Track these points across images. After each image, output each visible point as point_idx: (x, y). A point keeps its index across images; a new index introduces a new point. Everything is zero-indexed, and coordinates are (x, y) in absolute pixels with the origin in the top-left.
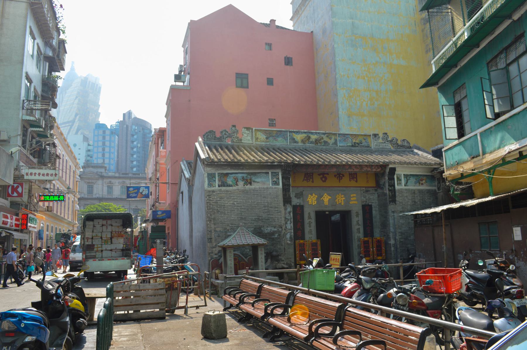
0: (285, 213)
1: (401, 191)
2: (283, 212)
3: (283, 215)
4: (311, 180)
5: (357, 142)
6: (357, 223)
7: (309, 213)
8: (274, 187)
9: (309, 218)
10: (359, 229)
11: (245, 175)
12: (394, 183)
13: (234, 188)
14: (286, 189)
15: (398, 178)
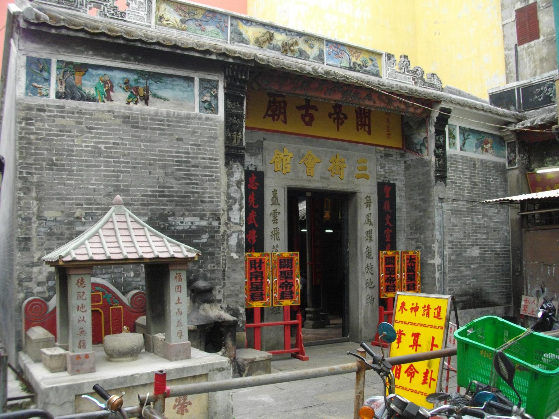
0: (229, 186)
1: (453, 157)
2: (224, 180)
3: (223, 188)
4: (282, 117)
5: (359, 62)
7: (275, 191)
8: (204, 115)
9: (275, 201)
10: (369, 233)
11: (132, 77)
12: (444, 141)
14: (232, 125)
15: (450, 133)
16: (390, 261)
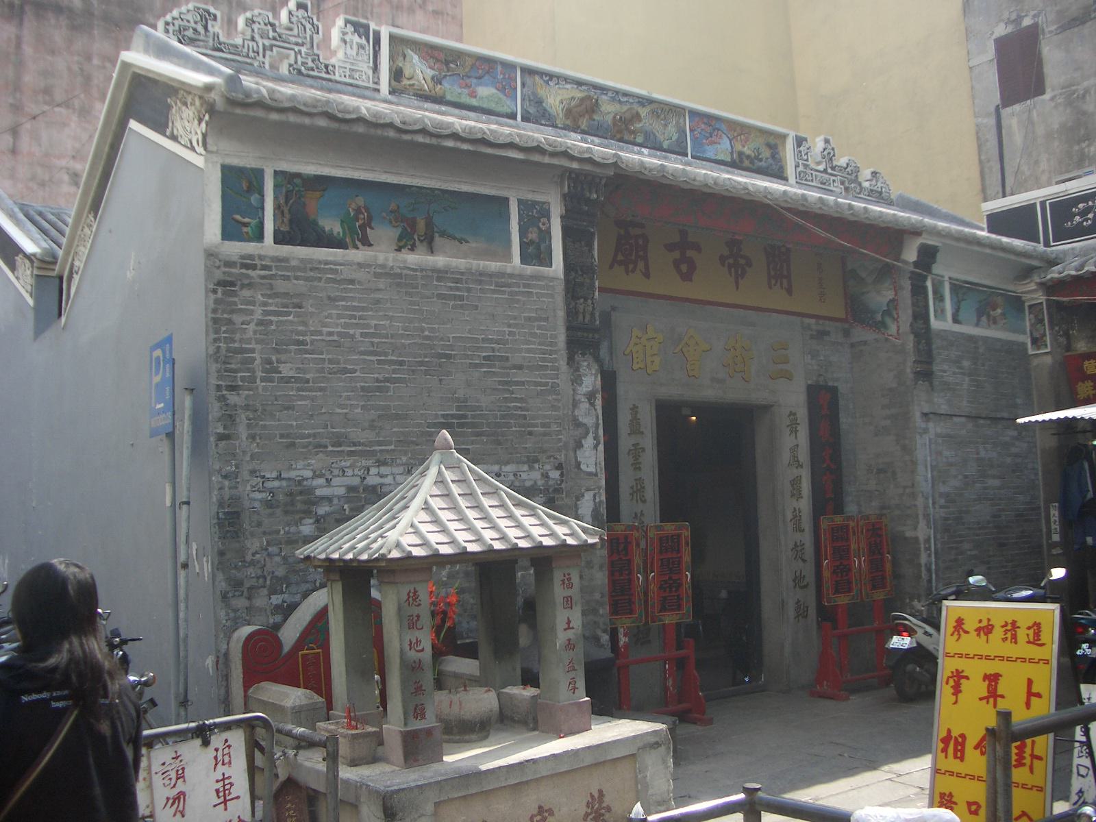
1: (943, 334)
4: (641, 265)
5: (747, 151)
6: (788, 456)
7: (634, 409)
8: (530, 269)
9: (635, 430)
10: (796, 482)
13: (356, 255)
16: (840, 534)
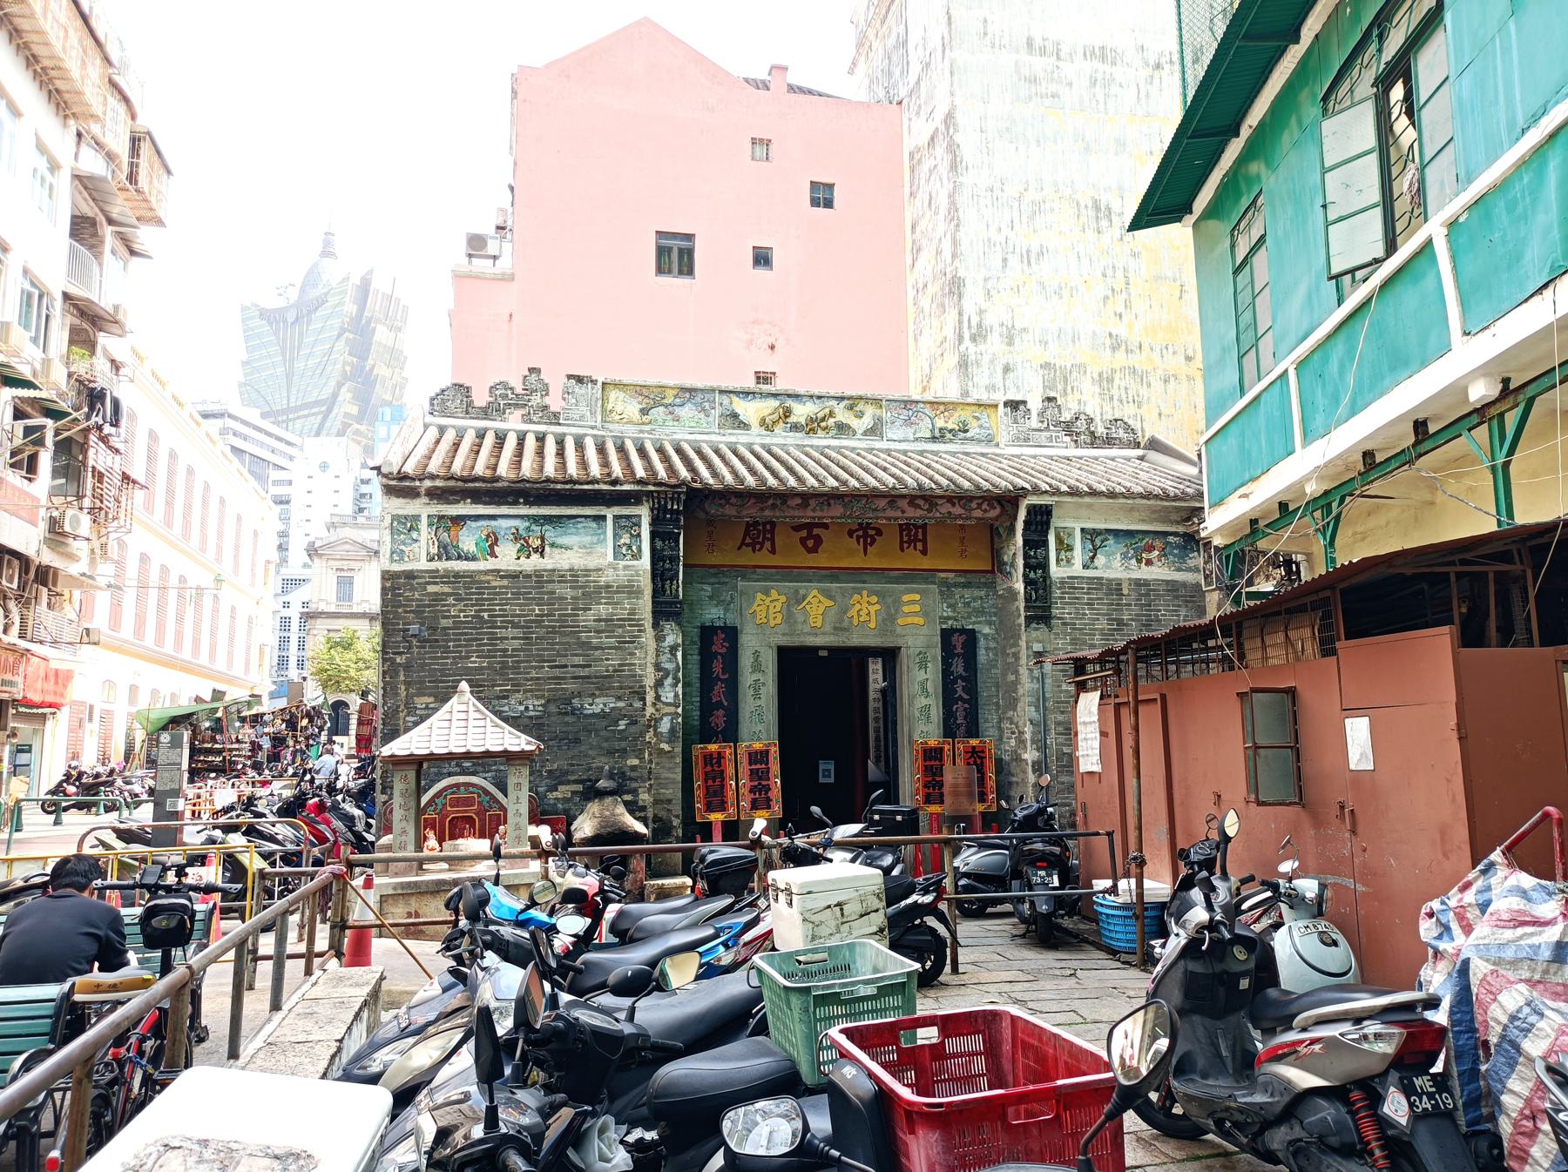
0: (658, 652)
1: (1070, 583)
2: (652, 645)
3: (651, 659)
4: (768, 545)
7: (756, 654)
9: (757, 667)
11: (522, 525)
12: (1047, 558)
14: (661, 574)
15: (1060, 541)
